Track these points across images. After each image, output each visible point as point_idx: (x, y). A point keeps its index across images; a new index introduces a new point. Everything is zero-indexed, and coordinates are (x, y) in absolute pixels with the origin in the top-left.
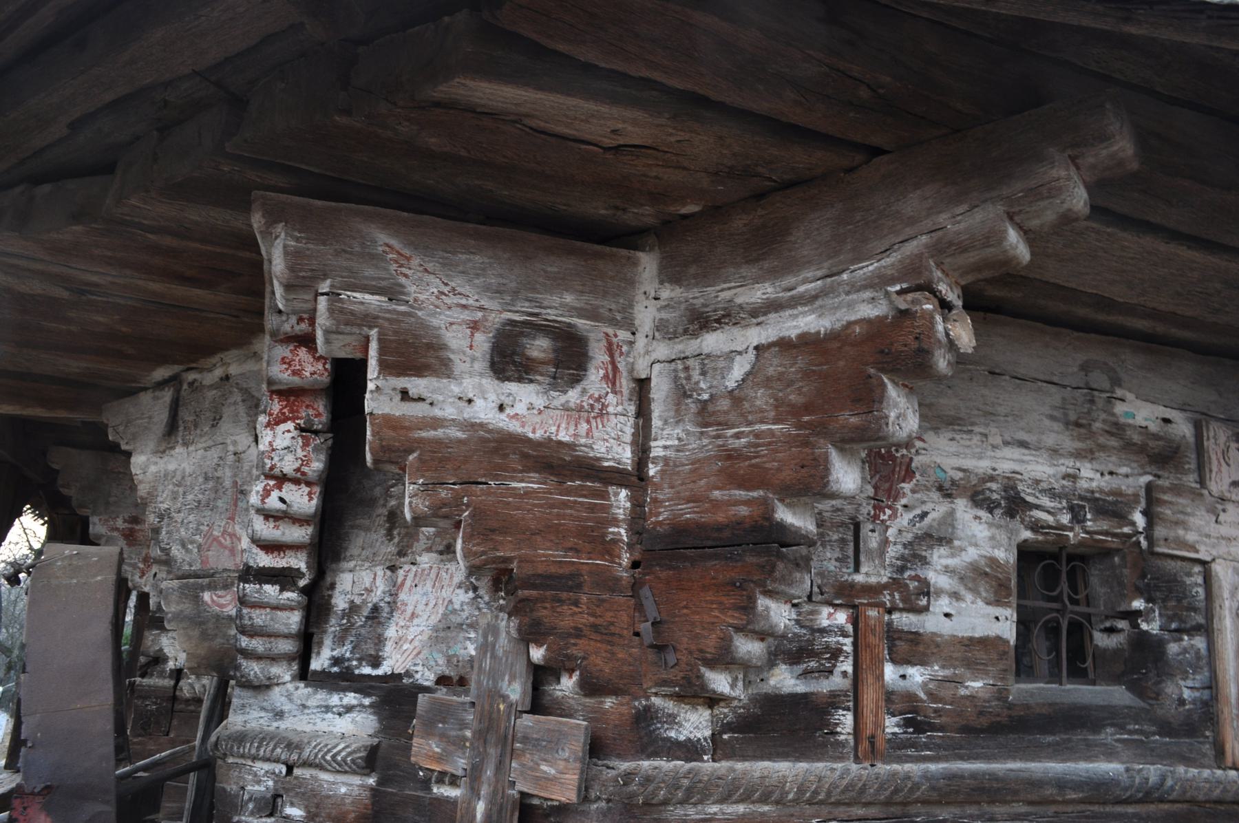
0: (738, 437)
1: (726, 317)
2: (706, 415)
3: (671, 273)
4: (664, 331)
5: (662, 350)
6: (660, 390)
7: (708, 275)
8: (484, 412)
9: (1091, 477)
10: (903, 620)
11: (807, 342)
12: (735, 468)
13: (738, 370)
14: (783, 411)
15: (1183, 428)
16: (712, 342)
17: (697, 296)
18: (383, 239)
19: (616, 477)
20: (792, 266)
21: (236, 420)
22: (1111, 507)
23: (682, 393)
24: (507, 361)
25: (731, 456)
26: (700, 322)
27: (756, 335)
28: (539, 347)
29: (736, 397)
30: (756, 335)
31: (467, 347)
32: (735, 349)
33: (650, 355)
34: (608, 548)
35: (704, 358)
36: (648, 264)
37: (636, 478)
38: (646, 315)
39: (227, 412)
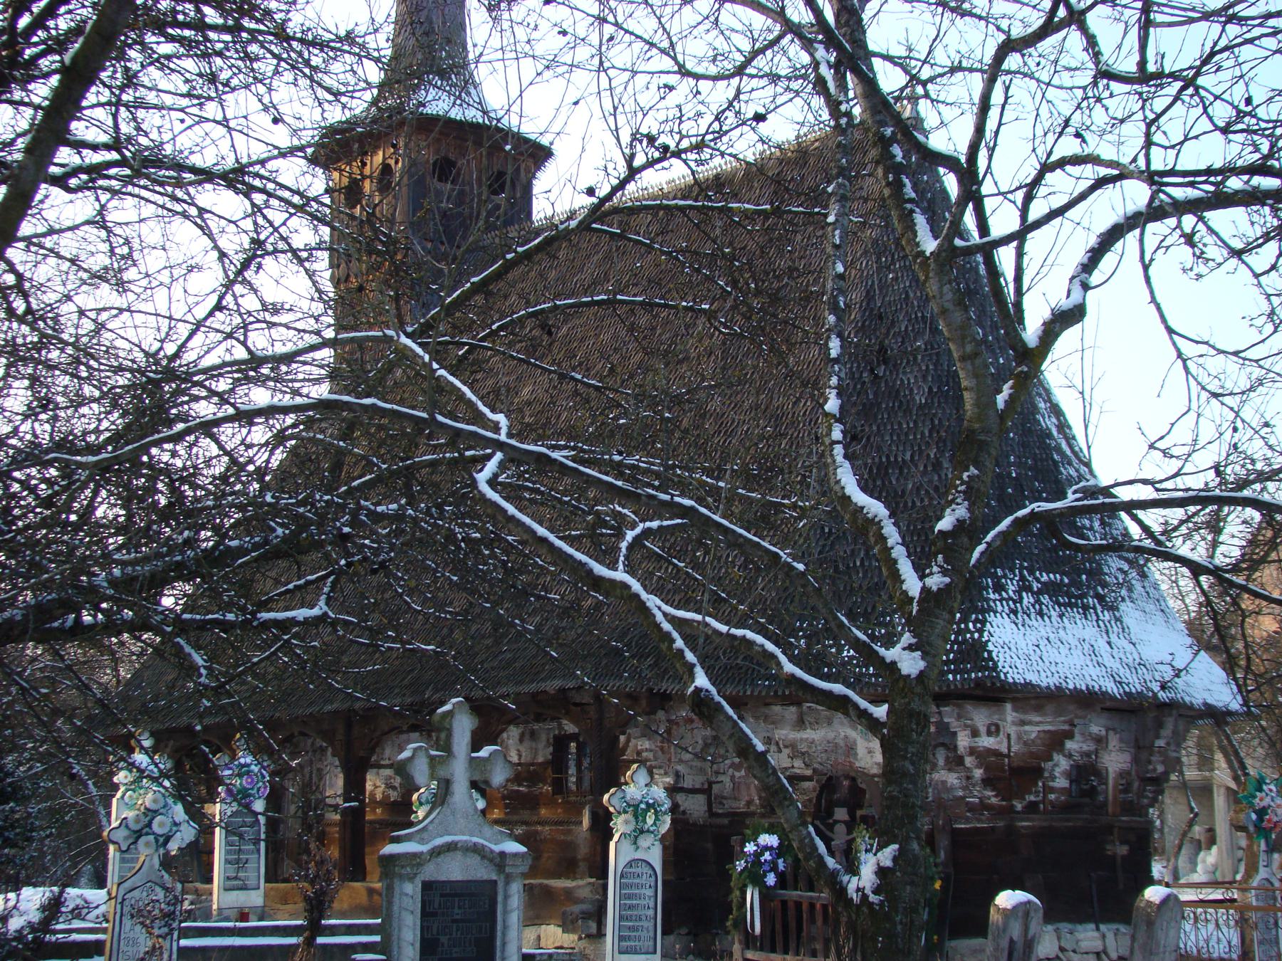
0: (1034, 749)
1: (1030, 723)
2: (1025, 743)
3: (1015, 709)
4: (1014, 723)
5: (1014, 728)
6: (1013, 737)
7: (1025, 712)
8: (986, 744)
9: (1085, 748)
10: (1051, 784)
11: (1049, 731)
12: (1032, 755)
13: (1034, 735)
14: (1044, 745)
15: (1103, 733)
16: (1027, 728)
17: (1022, 717)
18: (969, 707)
19: (1005, 756)
20: (1045, 715)
21: (842, 724)
22: (1088, 754)
23: (1019, 738)
24: (989, 733)
25: (1032, 753)
26: (1023, 723)
27: (1038, 728)
28: (993, 728)
29: (1033, 741)
30: (1038, 728)
31: (983, 730)
32: (1032, 731)
33: (1012, 730)
34: (1004, 771)
35: (1026, 732)
36: (1009, 706)
37: (1008, 756)
38: (1009, 719)
39: (835, 721)
